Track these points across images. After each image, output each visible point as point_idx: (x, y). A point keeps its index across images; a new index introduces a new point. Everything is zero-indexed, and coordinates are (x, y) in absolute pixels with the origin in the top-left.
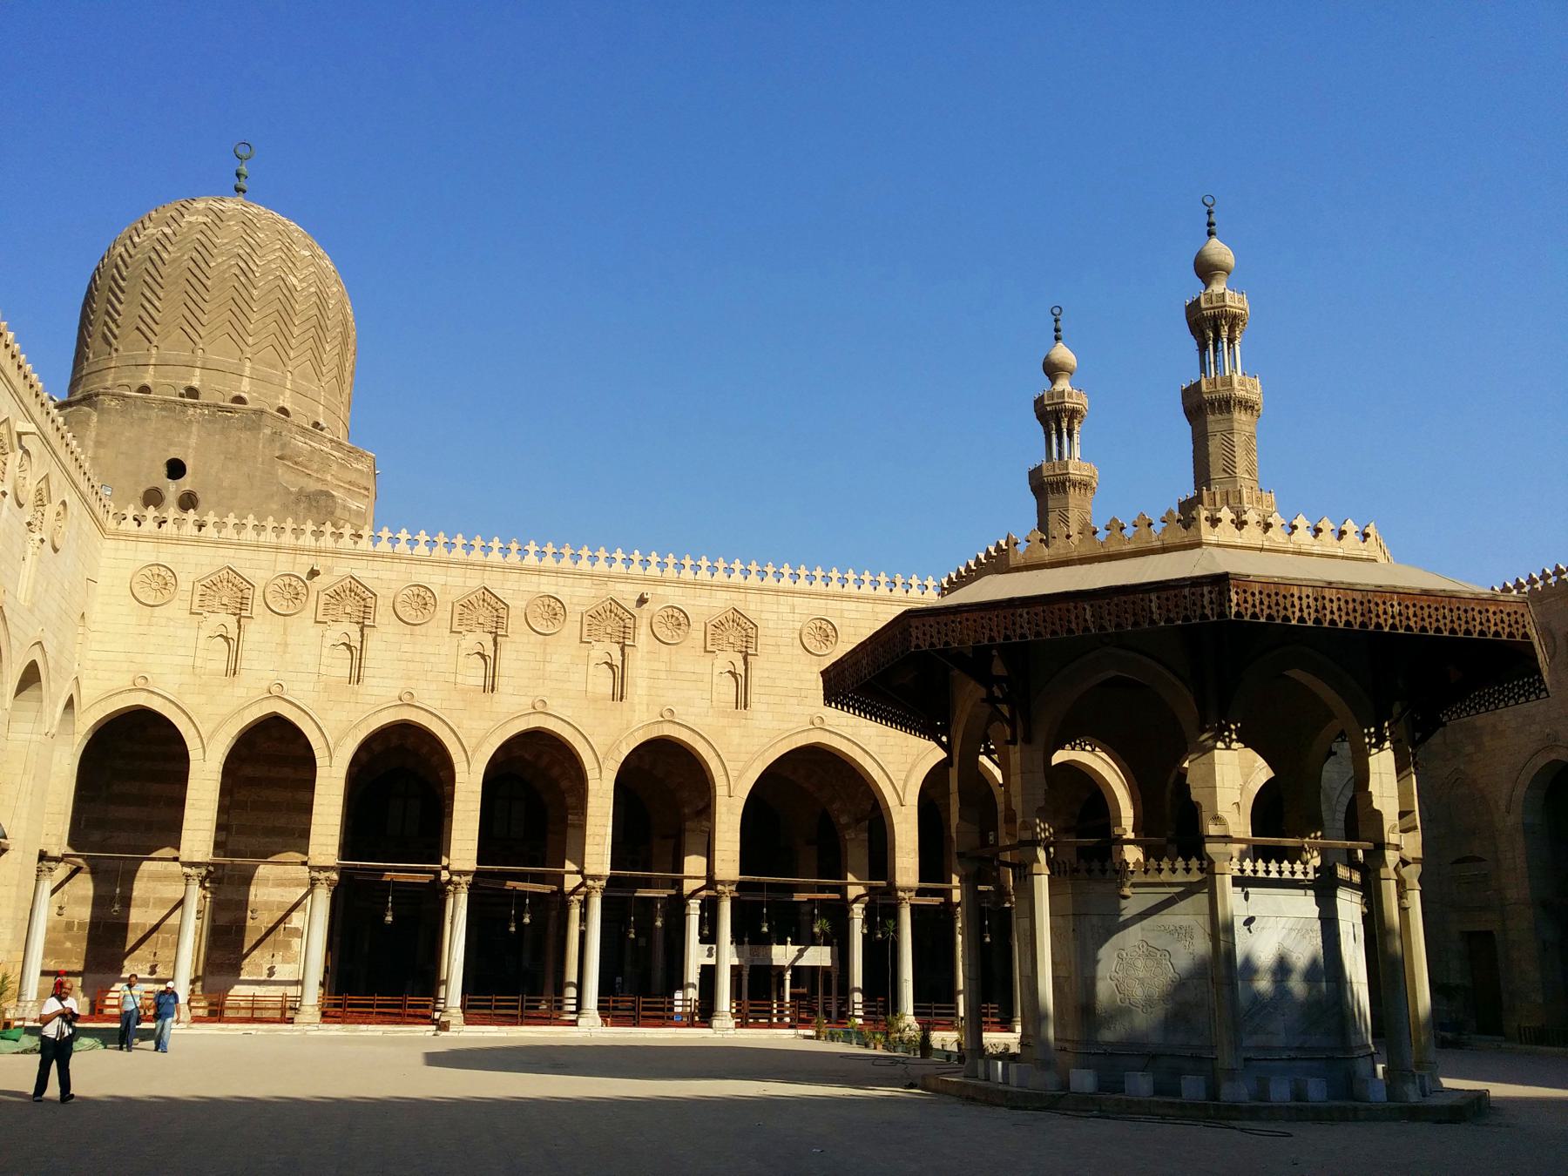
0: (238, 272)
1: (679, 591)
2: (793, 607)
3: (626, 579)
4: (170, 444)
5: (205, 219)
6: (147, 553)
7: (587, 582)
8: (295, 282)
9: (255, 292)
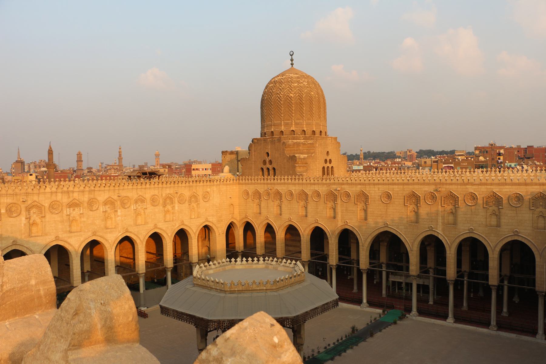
1: (348, 186)
2: (379, 188)
3: (334, 184)
6: (244, 187)
7: (325, 186)
8: (292, 95)
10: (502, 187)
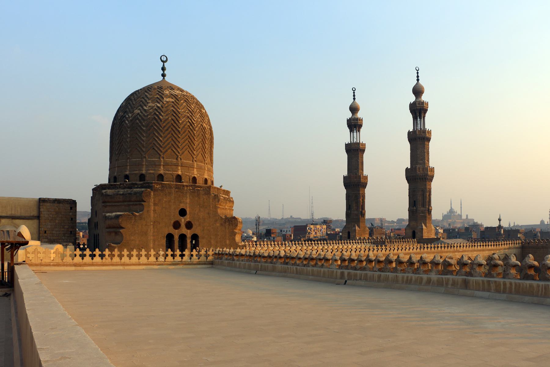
0: (189, 124)
4: (181, 202)
5: (173, 100)
9: (195, 132)
10: (472, 253)
